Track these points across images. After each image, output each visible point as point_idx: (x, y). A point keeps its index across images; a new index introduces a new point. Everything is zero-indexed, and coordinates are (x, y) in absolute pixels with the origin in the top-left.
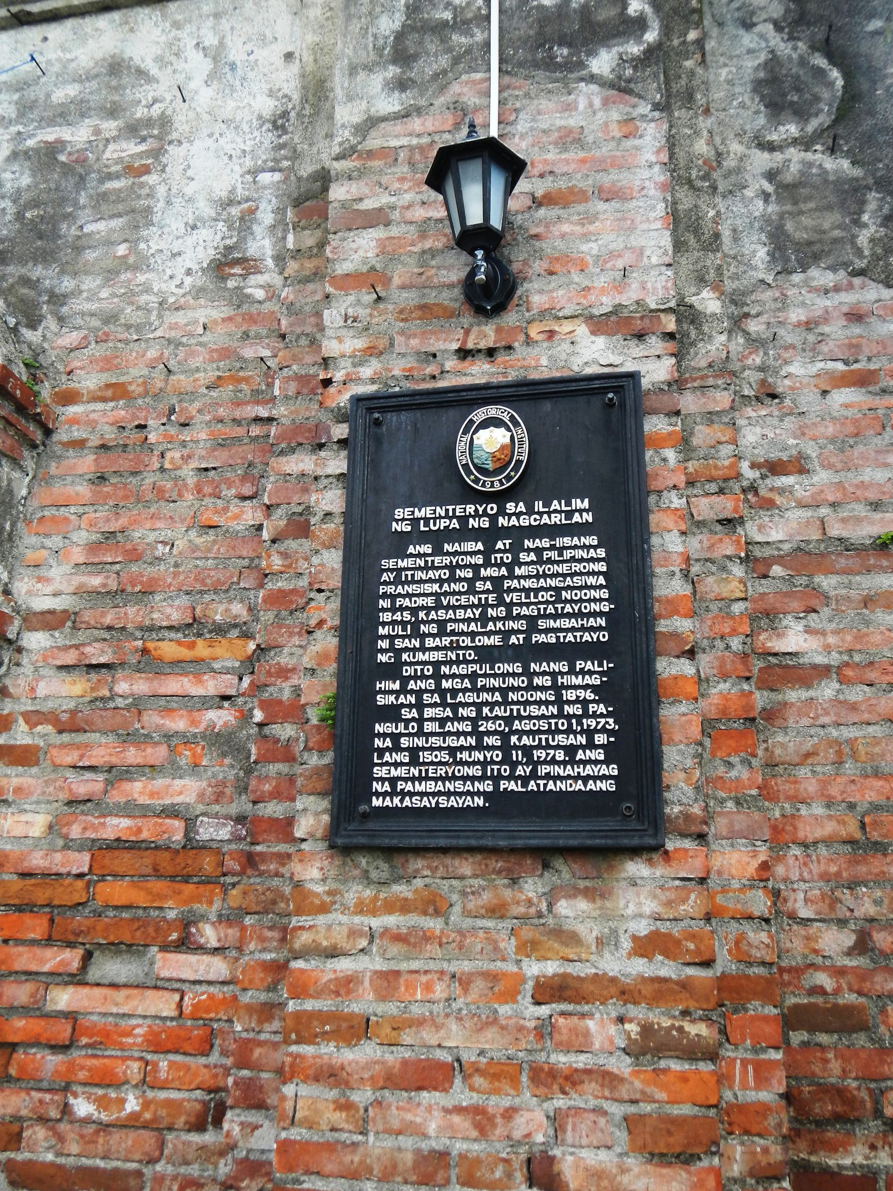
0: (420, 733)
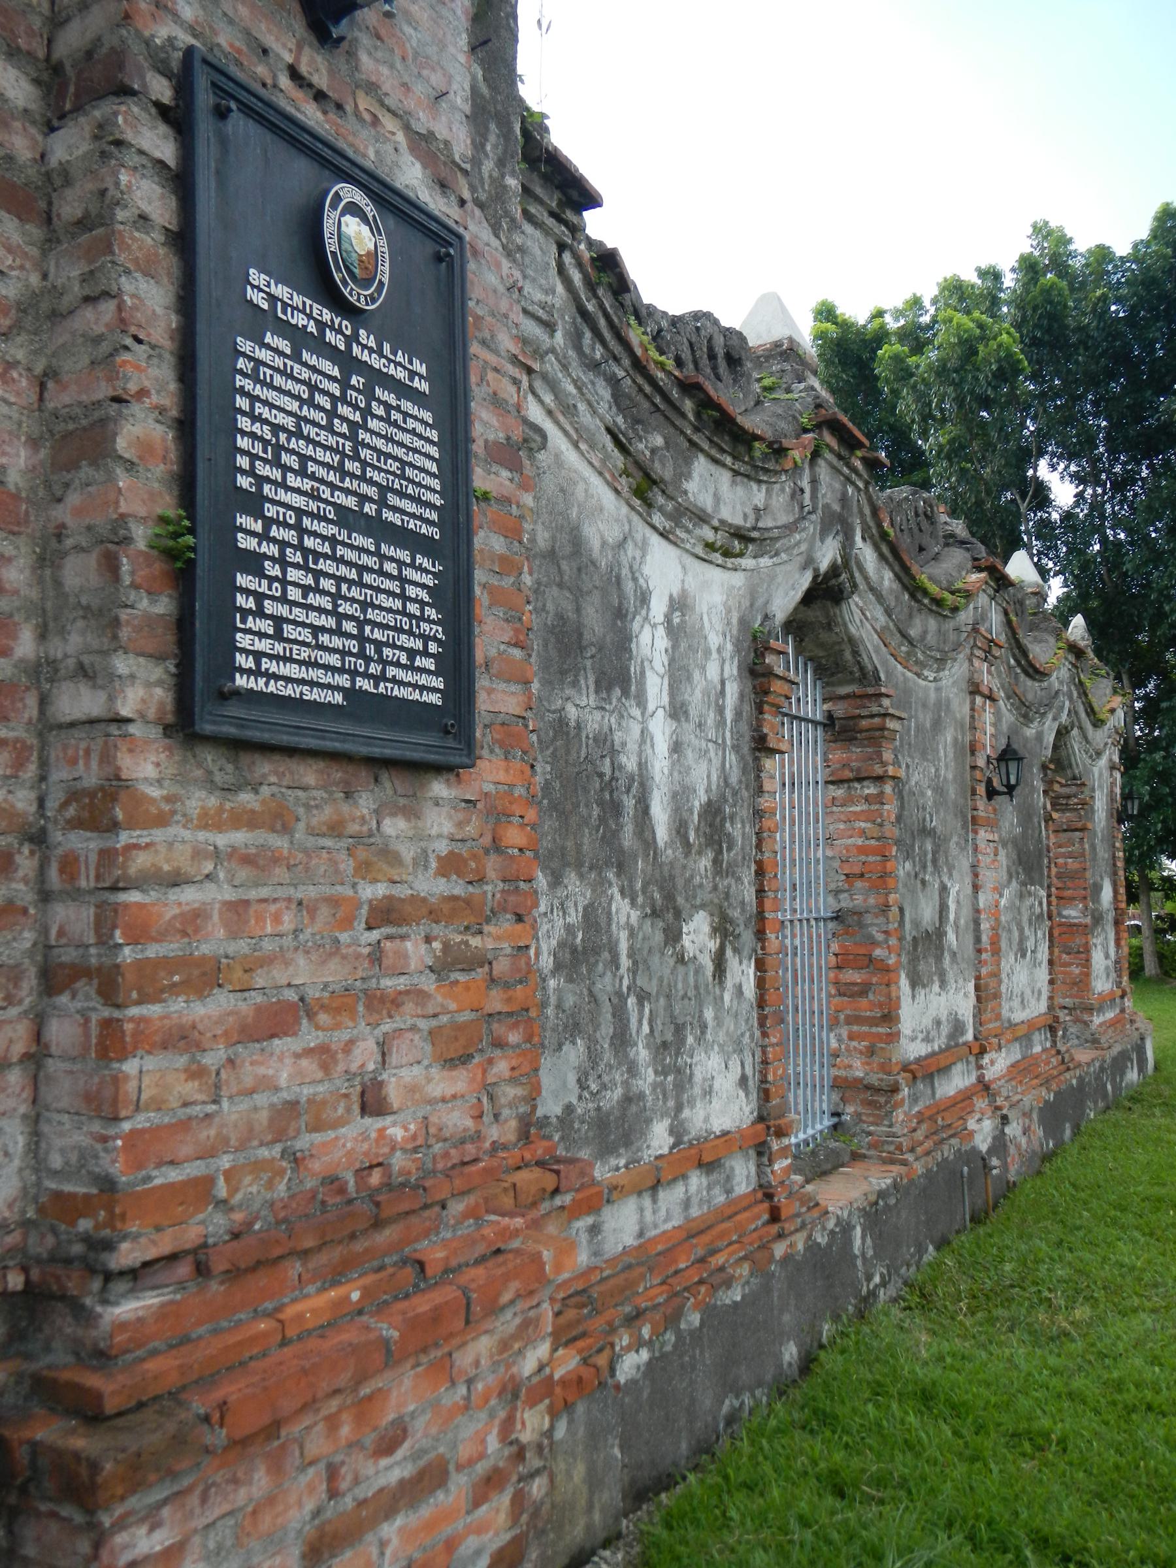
0: (283, 599)
